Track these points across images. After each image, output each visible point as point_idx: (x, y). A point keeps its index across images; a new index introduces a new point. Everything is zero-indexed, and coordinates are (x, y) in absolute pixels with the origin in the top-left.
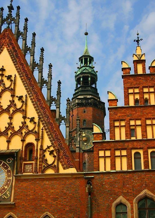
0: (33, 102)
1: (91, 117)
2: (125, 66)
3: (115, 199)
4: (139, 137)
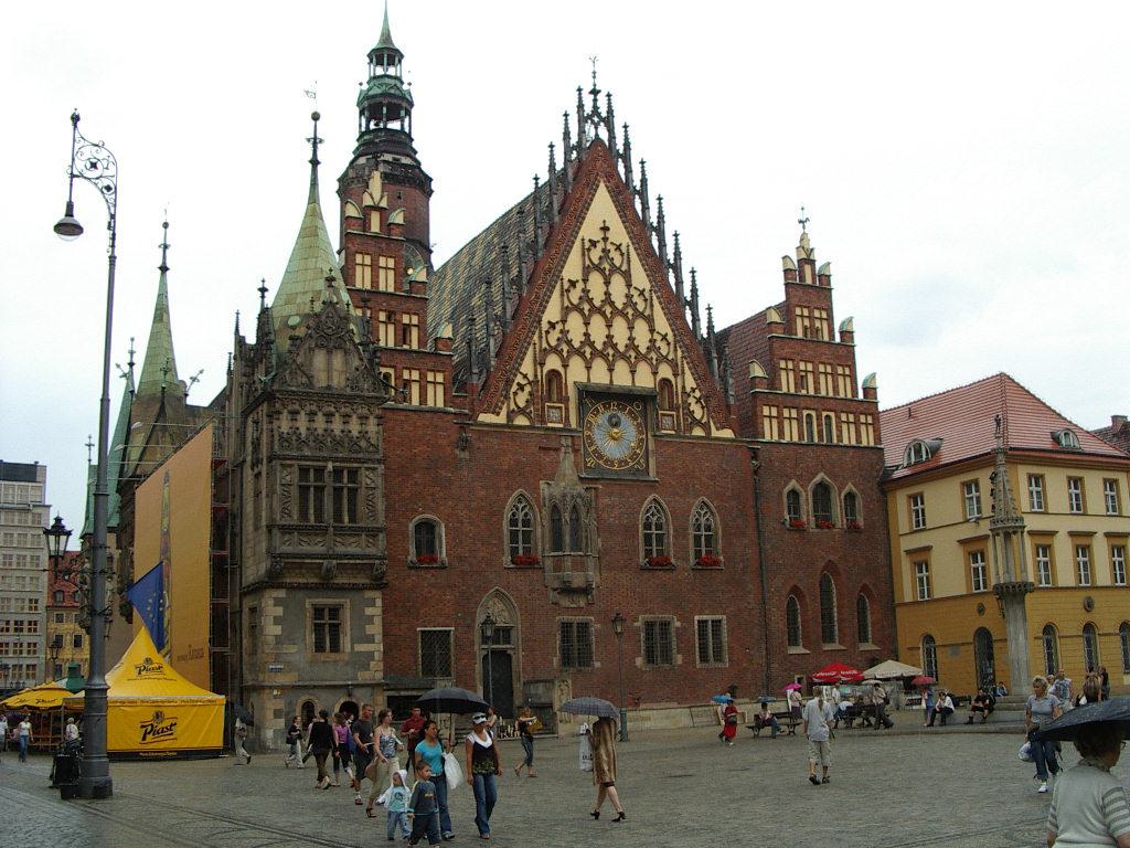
0: (660, 303)
2: (790, 266)
3: (786, 484)
4: (812, 392)
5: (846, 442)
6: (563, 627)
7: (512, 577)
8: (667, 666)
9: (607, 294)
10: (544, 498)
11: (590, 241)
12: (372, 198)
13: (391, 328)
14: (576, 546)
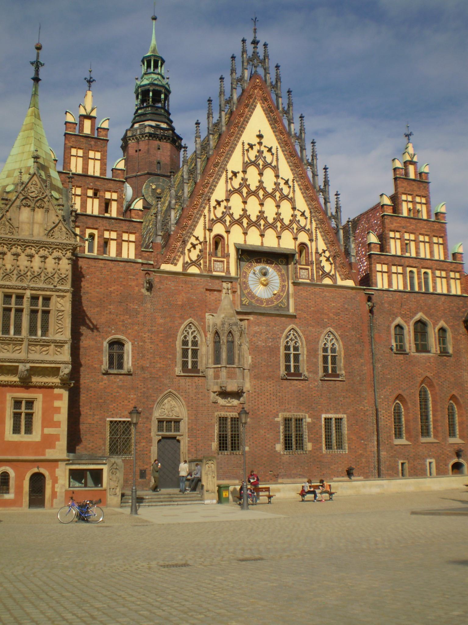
0: (301, 189)
1: (168, 159)
3: (394, 320)
4: (414, 255)
5: (439, 291)
6: (220, 420)
7: (182, 381)
8: (299, 452)
9: (261, 182)
10: (209, 326)
11: (249, 144)
12: (85, 110)
13: (96, 201)
14: (231, 360)
